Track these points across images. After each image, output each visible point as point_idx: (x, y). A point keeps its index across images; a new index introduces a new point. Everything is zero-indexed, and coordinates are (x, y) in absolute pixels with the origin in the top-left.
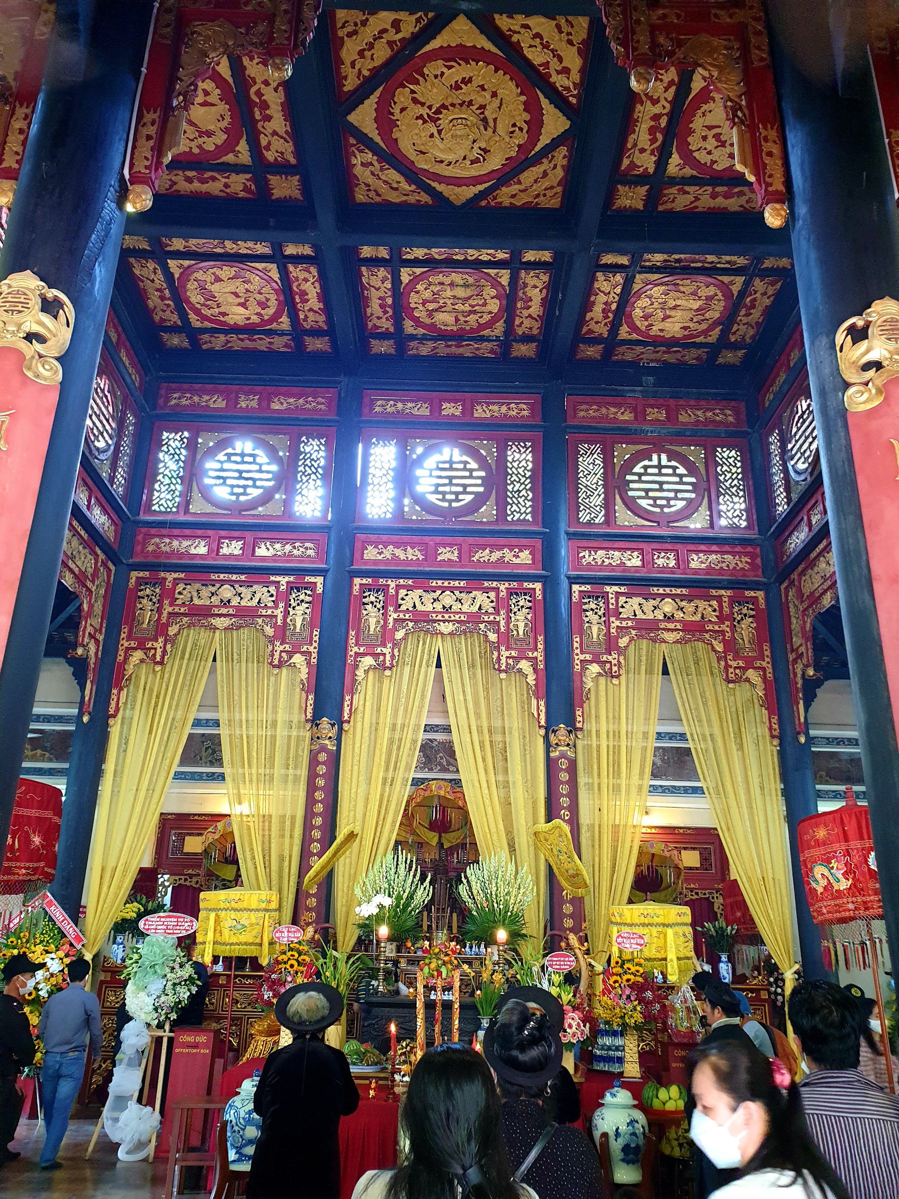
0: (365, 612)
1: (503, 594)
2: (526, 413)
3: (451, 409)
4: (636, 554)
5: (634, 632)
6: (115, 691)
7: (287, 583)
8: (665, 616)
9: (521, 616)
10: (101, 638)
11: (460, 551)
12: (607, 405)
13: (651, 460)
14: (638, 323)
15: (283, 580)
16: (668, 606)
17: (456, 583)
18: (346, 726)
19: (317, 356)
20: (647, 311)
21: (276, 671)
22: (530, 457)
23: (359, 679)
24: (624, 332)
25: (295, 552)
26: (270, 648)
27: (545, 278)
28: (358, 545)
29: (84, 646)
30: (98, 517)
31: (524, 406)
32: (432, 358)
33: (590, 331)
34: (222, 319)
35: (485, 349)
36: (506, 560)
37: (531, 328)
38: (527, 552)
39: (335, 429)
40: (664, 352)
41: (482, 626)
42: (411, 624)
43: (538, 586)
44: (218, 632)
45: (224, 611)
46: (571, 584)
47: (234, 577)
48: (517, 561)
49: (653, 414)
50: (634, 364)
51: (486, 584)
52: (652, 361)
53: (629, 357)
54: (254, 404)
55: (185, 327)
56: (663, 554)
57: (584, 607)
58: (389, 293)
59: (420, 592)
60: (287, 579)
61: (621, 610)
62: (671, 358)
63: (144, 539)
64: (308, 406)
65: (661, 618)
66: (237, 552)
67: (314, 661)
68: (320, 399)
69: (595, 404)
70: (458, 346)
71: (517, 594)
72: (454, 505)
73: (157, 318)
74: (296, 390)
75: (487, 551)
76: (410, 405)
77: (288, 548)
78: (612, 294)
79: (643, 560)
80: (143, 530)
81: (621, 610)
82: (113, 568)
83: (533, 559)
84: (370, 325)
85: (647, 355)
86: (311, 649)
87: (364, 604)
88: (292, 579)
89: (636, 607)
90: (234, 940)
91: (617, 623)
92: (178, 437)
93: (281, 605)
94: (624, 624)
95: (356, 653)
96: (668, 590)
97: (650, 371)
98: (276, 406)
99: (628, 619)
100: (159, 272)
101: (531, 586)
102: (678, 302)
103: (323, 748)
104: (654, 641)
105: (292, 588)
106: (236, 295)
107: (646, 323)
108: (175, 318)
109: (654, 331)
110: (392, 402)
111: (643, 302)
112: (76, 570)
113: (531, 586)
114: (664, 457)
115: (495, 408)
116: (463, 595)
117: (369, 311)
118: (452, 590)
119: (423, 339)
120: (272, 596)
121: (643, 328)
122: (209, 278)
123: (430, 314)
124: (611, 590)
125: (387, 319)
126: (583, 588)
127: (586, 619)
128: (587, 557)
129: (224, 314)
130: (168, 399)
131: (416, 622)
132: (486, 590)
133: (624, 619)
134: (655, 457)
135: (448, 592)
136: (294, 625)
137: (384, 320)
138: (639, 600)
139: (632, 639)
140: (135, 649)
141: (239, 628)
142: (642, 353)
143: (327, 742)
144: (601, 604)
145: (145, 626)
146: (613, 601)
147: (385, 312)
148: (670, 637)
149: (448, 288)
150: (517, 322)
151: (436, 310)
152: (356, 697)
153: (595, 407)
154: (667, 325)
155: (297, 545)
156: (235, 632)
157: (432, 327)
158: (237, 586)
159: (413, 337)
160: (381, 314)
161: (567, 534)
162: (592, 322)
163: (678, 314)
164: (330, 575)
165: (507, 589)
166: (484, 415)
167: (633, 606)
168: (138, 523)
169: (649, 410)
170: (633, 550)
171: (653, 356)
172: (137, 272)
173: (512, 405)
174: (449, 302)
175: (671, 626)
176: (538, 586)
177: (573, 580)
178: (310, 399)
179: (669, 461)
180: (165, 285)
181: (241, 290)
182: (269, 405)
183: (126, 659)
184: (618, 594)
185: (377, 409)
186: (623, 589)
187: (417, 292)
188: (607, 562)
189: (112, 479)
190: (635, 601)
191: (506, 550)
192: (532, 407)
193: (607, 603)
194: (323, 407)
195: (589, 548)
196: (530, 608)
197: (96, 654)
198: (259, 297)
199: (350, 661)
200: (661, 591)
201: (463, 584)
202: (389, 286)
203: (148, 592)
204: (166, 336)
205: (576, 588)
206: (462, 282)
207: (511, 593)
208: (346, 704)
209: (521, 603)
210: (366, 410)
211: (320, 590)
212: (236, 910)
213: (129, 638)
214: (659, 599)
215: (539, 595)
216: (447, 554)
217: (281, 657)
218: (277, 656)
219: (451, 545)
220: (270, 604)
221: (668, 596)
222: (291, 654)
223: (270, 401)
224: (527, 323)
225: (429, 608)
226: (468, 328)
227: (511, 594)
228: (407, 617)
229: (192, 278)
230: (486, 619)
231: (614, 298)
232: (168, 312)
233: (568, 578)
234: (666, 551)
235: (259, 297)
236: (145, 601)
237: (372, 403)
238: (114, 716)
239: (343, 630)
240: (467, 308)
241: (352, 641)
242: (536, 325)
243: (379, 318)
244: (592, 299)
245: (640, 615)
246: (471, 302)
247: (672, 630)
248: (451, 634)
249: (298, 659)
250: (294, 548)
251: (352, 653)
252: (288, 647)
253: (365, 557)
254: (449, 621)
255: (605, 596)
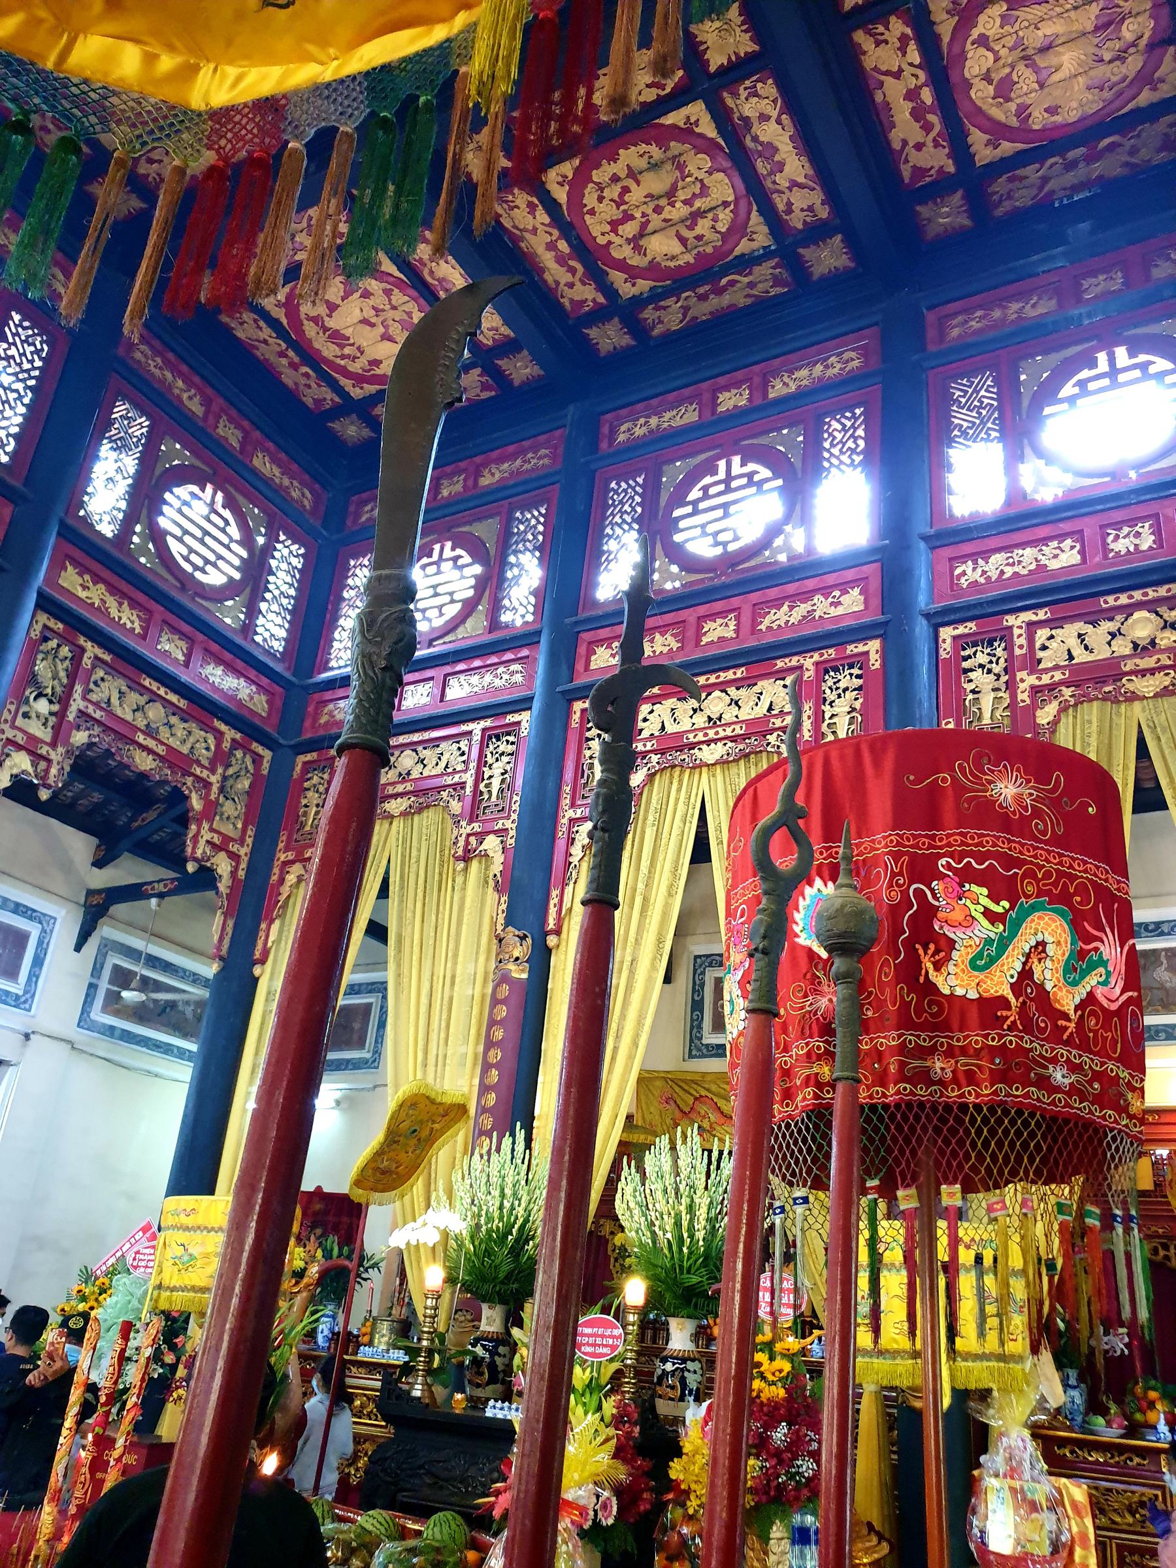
0: (588, 753)
1: (809, 675)
2: (856, 363)
3: (731, 400)
4: (1068, 542)
5: (1067, 692)
6: (263, 926)
7: (484, 730)
8: (1136, 646)
9: (842, 706)
10: (243, 851)
11: (738, 618)
12: (1002, 302)
13: (1093, 364)
14: (997, 114)
15: (476, 728)
16: (1142, 626)
17: (729, 675)
18: (552, 940)
19: (532, 388)
20: (996, 77)
21: (461, 865)
22: (860, 432)
23: (574, 860)
24: (983, 150)
25: (498, 683)
26: (455, 832)
27: (768, 89)
28: (582, 650)
29: (196, 860)
30: (219, 679)
31: (853, 354)
32: (694, 331)
33: (919, 172)
34: (378, 372)
35: (764, 279)
36: (817, 614)
37: (811, 209)
38: (857, 591)
39: (557, 486)
40: (1089, 159)
41: (772, 738)
42: (655, 758)
43: (874, 646)
44: (395, 823)
45: (400, 788)
46: (936, 628)
47: (416, 737)
48: (840, 611)
49: (1095, 286)
50: (1043, 208)
51: (780, 664)
52: (1075, 189)
53: (1023, 198)
54: (459, 487)
55: (348, 407)
56: (1126, 530)
57: (965, 665)
58: (556, 233)
59: (671, 702)
60: (483, 724)
61: (1040, 654)
62: (1109, 167)
63: (316, 709)
64: (527, 466)
65: (1128, 651)
66: (425, 700)
67: (511, 842)
68: (543, 452)
69: (980, 307)
70: (720, 291)
71: (836, 670)
72: (731, 548)
73: (309, 401)
74: (511, 449)
75: (785, 608)
76: (668, 415)
77: (488, 678)
78: (908, 70)
79: (1082, 552)
80: (316, 696)
81: (1040, 654)
82: (267, 754)
83: (866, 602)
84: (566, 302)
85: (1057, 178)
86: (508, 824)
87: (588, 739)
88: (488, 723)
89: (1073, 643)
90: (175, 1282)
91: (1032, 680)
92: (366, 562)
93: (473, 765)
94: (1046, 679)
95: (571, 820)
96: (1138, 595)
97: (1077, 211)
98: (485, 481)
99: (1056, 667)
100: (262, 323)
101: (861, 648)
102: (1048, 29)
103: (505, 978)
104: (1112, 699)
105: (490, 738)
106: (365, 322)
107: (1012, 107)
108: (328, 395)
109: (1039, 119)
110: (642, 421)
111: (977, 62)
112: (161, 750)
113: (861, 648)
114: (1121, 352)
115: (804, 373)
116: (743, 692)
117: (547, 276)
118: (723, 687)
119: (655, 298)
120: (463, 754)
121: (1014, 122)
122: (322, 310)
123: (635, 242)
124: (1016, 622)
125: (584, 284)
126: (961, 630)
127: (969, 687)
128: (969, 573)
129: (376, 363)
130: (358, 515)
131: (662, 752)
132: (780, 675)
133: (1046, 670)
134: (1102, 357)
135: (717, 693)
136: (490, 792)
137: (578, 285)
138: (1079, 626)
139: (1063, 709)
140: (292, 862)
141: (420, 811)
142: (1045, 180)
143: (511, 966)
144: (999, 652)
145: (308, 828)
146: (1023, 641)
147: (573, 271)
148: (1147, 686)
149: (631, 184)
150: (781, 207)
151: (642, 234)
152: (569, 890)
153: (979, 313)
154: (1058, 92)
155: (501, 669)
156: (416, 818)
157: (653, 270)
158: (420, 748)
159: (639, 302)
160: (568, 277)
161: (925, 538)
162: (909, 149)
163: (1068, 60)
164: (536, 705)
165: (817, 664)
166: (785, 391)
167: (1066, 643)
168: (306, 688)
169: (1086, 284)
170: (1061, 537)
171: (1071, 178)
172: (240, 334)
173: (833, 359)
174: (649, 211)
175: (1148, 662)
176: (874, 646)
177: (938, 620)
178: (530, 455)
179: (1132, 354)
180: (284, 346)
181: (369, 314)
182: (476, 482)
183: (282, 881)
184: (1032, 627)
185: (621, 438)
186: (1042, 615)
187: (592, 212)
188: (1009, 571)
189: (248, 629)
190: (1069, 633)
191: (818, 598)
192: (865, 352)
193: (1009, 648)
194: (546, 461)
195: (973, 557)
196: (859, 689)
197: (233, 874)
198: (398, 315)
199: (562, 833)
200: (1124, 599)
201: (740, 673)
202: (547, 220)
203: (316, 780)
204: (335, 425)
205: (946, 633)
206: (643, 163)
207: (823, 669)
208: (552, 903)
209: (842, 685)
210: (604, 445)
211: (524, 732)
212: (187, 1229)
213: (287, 849)
214: (1119, 618)
215: (875, 662)
216: (718, 631)
217: (467, 843)
218: (461, 843)
219: (723, 614)
220: (460, 767)
221: (1140, 606)
222: (481, 836)
223: (478, 474)
224: (800, 200)
225: (686, 725)
226: (709, 250)
227: (826, 672)
228: (649, 748)
229: (303, 316)
230: (778, 723)
231: (916, 78)
232: (314, 385)
233: (927, 616)
234: (1132, 522)
235: (398, 315)
236: (310, 794)
237: (613, 432)
238: (263, 961)
239: (551, 785)
240: (679, 211)
241: (566, 801)
242: (816, 197)
243: (571, 285)
244: (879, 97)
245: (1081, 656)
246: (682, 195)
247: (1153, 671)
248: (723, 762)
249: (491, 843)
250: (496, 676)
251: (565, 821)
252: (477, 827)
253: (593, 666)
254: (715, 741)
255: (1006, 635)
